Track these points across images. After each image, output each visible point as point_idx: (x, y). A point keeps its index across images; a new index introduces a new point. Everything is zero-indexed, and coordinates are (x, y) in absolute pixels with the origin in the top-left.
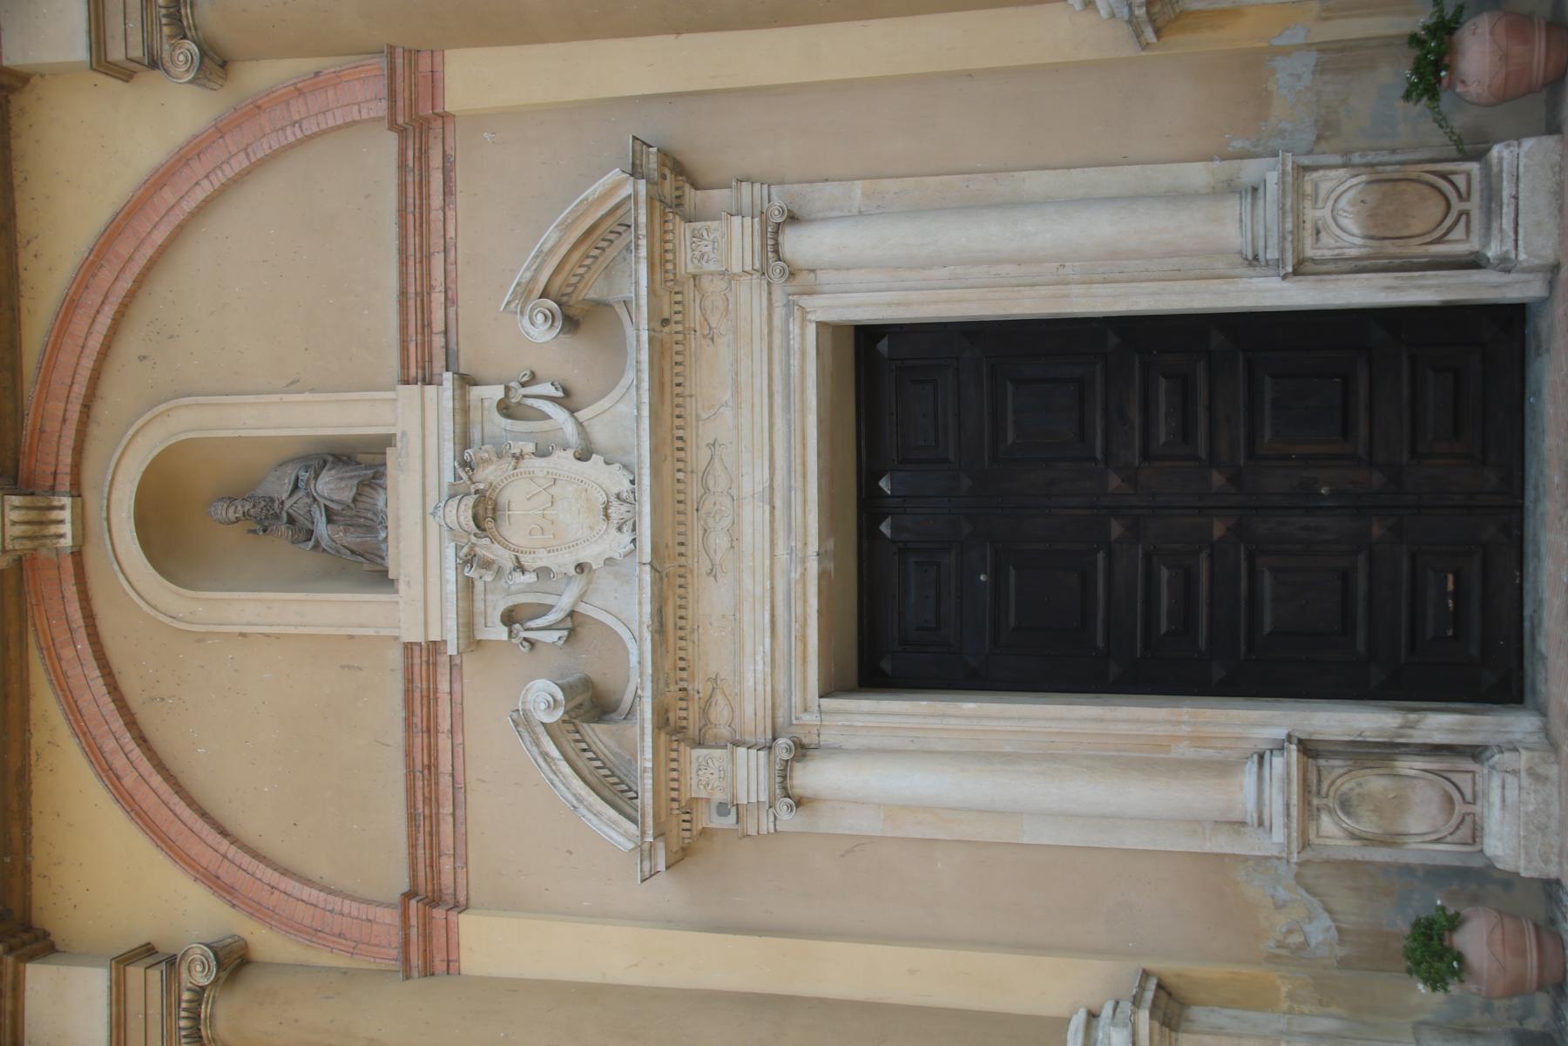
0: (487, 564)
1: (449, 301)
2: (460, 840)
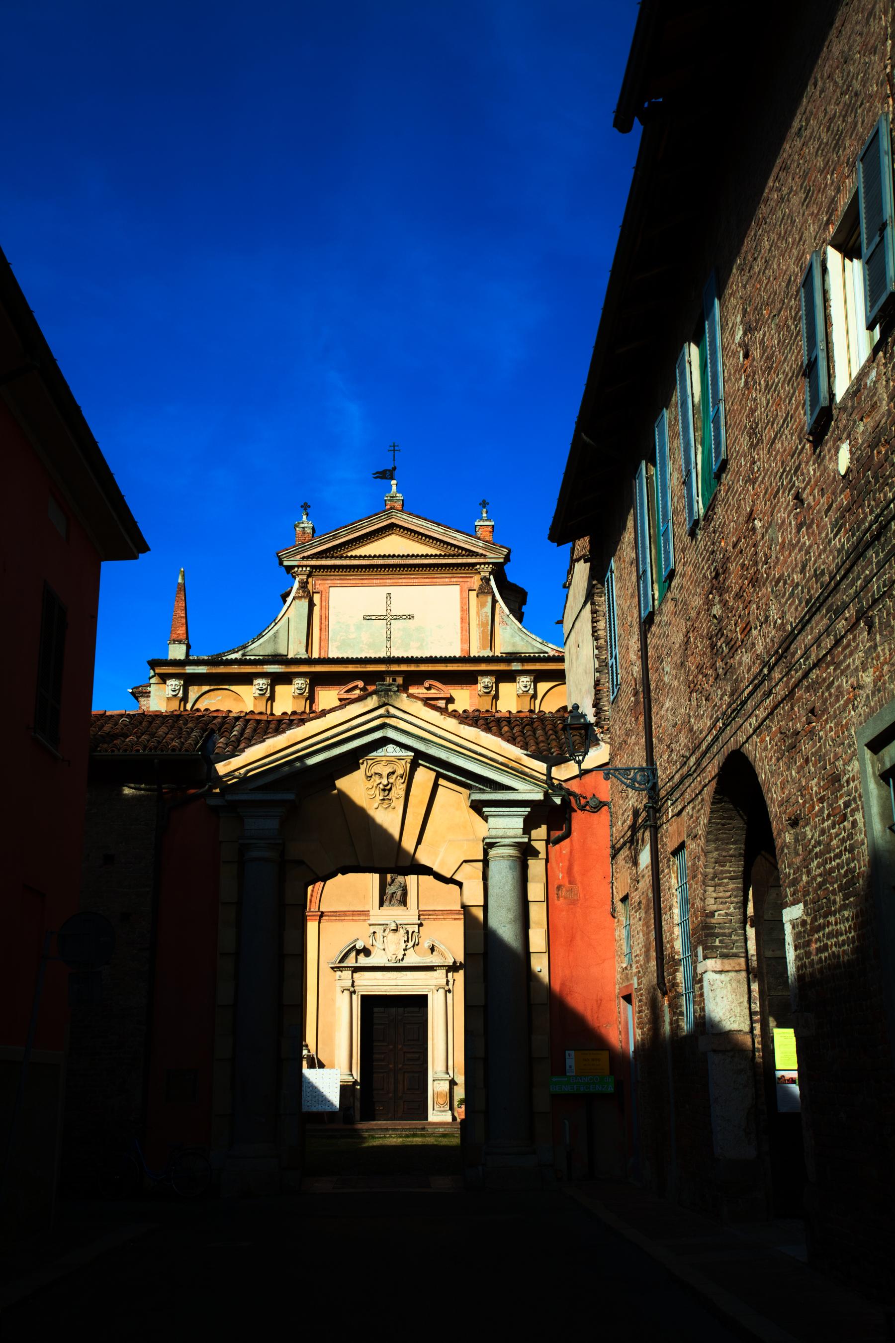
0: (385, 931)
1: (435, 919)
2: (331, 921)
